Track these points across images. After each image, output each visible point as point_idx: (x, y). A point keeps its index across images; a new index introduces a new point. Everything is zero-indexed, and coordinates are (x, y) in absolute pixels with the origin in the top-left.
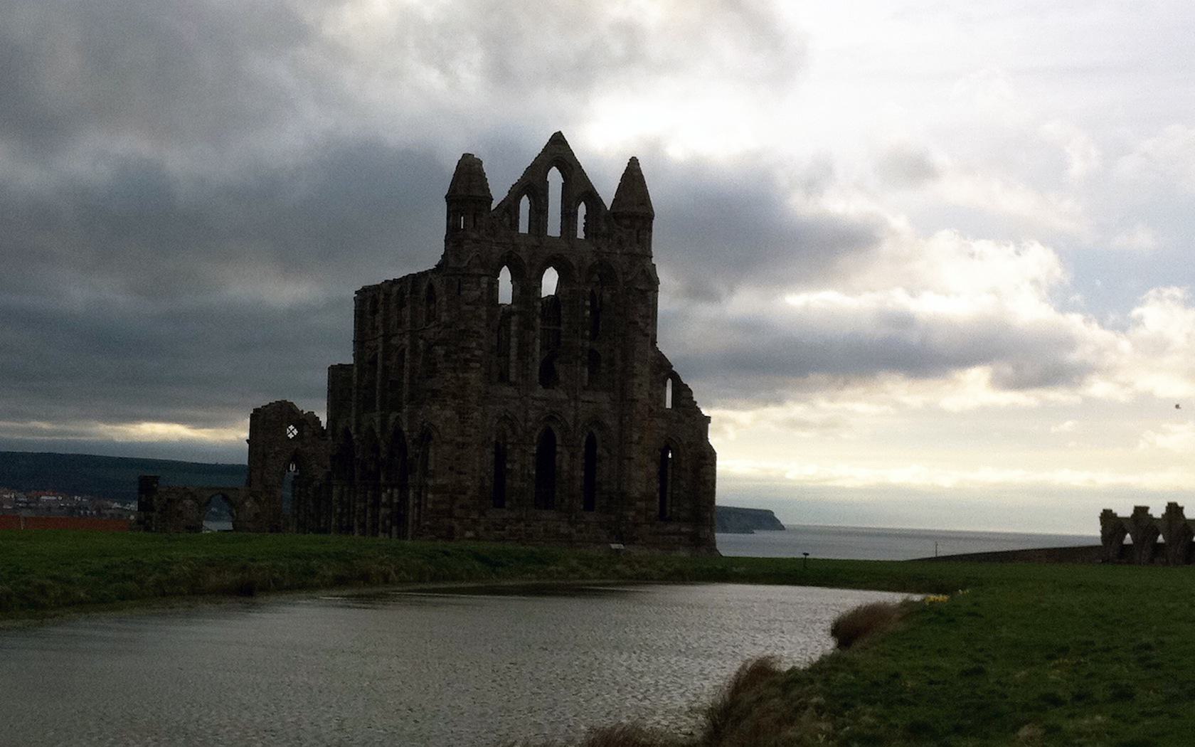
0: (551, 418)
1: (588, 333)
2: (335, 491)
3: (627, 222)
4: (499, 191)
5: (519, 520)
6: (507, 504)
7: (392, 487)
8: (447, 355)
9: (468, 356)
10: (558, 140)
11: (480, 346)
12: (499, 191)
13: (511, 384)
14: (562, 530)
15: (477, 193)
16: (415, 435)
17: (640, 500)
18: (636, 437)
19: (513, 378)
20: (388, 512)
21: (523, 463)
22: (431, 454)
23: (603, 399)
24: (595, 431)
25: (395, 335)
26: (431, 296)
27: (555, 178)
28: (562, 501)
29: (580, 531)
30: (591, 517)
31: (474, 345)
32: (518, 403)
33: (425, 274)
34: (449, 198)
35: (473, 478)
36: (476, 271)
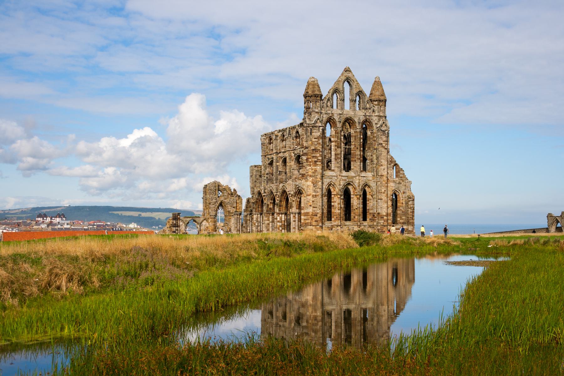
0: (349, 184)
1: (362, 149)
2: (255, 217)
3: (376, 103)
4: (325, 91)
5: (337, 226)
6: (333, 219)
7: (282, 214)
8: (307, 160)
9: (316, 160)
10: (347, 70)
13: (333, 170)
15: (317, 92)
16: (292, 193)
18: (383, 191)
19: (333, 169)
20: (281, 224)
21: (337, 202)
22: (302, 200)
23: (369, 175)
24: (366, 188)
25: (280, 153)
26: (298, 136)
28: (354, 217)
30: (365, 223)
31: (318, 155)
32: (336, 178)
33: (294, 128)
34: (305, 96)
36: (317, 125)
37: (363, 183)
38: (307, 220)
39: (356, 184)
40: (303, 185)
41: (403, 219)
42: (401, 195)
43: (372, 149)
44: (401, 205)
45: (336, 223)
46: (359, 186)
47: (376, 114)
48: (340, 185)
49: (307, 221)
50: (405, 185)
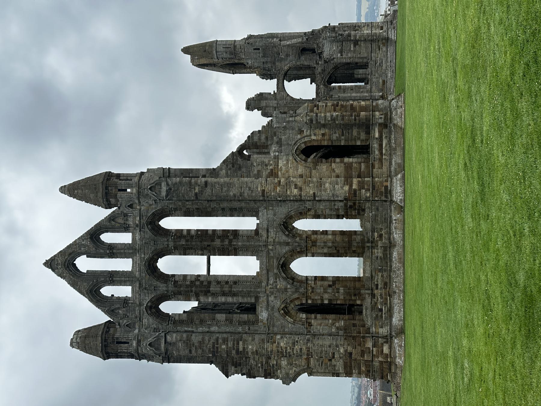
3: (113, 201)
5: (373, 296)
6: (358, 302)
9: (234, 352)
11: (225, 341)
12: (101, 317)
13: (257, 298)
14: (380, 255)
17: (351, 186)
18: (295, 191)
19: (253, 300)
27: (84, 264)
29: (381, 236)
31: (224, 347)
35: (337, 346)
36: (163, 345)
37: (281, 233)
38: (360, 368)
39: (285, 249)
40: (287, 374)
41: (359, 134)
42: (306, 139)
43: (209, 209)
44: (326, 137)
45: (368, 300)
46: (288, 244)
47: (137, 201)
48: (286, 289)
49: (363, 369)
50: (285, 128)
